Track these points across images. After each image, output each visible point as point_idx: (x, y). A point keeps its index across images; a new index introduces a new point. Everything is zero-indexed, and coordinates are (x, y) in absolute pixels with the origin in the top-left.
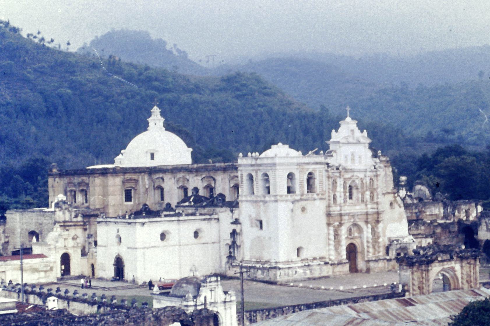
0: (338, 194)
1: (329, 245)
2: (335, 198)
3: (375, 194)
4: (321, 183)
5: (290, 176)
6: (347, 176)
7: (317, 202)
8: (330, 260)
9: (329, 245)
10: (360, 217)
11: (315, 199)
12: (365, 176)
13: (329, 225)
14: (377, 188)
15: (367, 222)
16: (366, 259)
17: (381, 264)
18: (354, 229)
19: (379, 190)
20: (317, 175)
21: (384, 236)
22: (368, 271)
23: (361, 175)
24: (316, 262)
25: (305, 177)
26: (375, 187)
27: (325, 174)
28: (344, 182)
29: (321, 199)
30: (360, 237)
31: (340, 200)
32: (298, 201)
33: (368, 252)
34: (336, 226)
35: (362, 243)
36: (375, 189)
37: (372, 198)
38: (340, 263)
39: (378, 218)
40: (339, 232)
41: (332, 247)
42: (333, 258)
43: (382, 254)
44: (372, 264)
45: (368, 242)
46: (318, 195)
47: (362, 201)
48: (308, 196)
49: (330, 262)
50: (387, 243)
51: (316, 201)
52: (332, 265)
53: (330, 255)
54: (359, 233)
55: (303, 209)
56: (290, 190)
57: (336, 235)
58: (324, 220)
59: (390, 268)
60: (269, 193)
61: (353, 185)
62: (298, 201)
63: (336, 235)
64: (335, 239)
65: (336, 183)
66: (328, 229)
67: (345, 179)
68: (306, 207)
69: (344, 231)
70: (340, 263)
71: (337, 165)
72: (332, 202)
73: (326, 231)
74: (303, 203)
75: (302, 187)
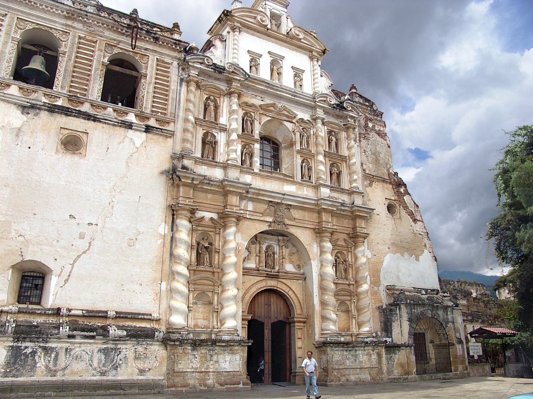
0: (221, 138)
1: (173, 274)
2: (209, 144)
4: (162, 91)
7: (138, 137)
9: (173, 274)
11: (129, 126)
13: (173, 211)
15: (319, 232)
16: (317, 337)
17: (365, 358)
21: (376, 282)
22: (324, 379)
23: (303, 115)
29: (148, 129)
30: (304, 278)
33: (324, 318)
35: (308, 295)
37: (336, 176)
38: (208, 343)
39: (354, 228)
42: (178, 320)
43: (369, 326)
44: (336, 355)
45: (323, 289)
46: (141, 116)
50: (385, 300)
53: (171, 310)
54: (299, 267)
57: (205, 252)
59: (396, 372)
62: (53, 109)
63: (205, 252)
65: (216, 107)
66: (173, 226)
68: (84, 137)
70: (208, 343)
73: (164, 229)
74: (76, 124)
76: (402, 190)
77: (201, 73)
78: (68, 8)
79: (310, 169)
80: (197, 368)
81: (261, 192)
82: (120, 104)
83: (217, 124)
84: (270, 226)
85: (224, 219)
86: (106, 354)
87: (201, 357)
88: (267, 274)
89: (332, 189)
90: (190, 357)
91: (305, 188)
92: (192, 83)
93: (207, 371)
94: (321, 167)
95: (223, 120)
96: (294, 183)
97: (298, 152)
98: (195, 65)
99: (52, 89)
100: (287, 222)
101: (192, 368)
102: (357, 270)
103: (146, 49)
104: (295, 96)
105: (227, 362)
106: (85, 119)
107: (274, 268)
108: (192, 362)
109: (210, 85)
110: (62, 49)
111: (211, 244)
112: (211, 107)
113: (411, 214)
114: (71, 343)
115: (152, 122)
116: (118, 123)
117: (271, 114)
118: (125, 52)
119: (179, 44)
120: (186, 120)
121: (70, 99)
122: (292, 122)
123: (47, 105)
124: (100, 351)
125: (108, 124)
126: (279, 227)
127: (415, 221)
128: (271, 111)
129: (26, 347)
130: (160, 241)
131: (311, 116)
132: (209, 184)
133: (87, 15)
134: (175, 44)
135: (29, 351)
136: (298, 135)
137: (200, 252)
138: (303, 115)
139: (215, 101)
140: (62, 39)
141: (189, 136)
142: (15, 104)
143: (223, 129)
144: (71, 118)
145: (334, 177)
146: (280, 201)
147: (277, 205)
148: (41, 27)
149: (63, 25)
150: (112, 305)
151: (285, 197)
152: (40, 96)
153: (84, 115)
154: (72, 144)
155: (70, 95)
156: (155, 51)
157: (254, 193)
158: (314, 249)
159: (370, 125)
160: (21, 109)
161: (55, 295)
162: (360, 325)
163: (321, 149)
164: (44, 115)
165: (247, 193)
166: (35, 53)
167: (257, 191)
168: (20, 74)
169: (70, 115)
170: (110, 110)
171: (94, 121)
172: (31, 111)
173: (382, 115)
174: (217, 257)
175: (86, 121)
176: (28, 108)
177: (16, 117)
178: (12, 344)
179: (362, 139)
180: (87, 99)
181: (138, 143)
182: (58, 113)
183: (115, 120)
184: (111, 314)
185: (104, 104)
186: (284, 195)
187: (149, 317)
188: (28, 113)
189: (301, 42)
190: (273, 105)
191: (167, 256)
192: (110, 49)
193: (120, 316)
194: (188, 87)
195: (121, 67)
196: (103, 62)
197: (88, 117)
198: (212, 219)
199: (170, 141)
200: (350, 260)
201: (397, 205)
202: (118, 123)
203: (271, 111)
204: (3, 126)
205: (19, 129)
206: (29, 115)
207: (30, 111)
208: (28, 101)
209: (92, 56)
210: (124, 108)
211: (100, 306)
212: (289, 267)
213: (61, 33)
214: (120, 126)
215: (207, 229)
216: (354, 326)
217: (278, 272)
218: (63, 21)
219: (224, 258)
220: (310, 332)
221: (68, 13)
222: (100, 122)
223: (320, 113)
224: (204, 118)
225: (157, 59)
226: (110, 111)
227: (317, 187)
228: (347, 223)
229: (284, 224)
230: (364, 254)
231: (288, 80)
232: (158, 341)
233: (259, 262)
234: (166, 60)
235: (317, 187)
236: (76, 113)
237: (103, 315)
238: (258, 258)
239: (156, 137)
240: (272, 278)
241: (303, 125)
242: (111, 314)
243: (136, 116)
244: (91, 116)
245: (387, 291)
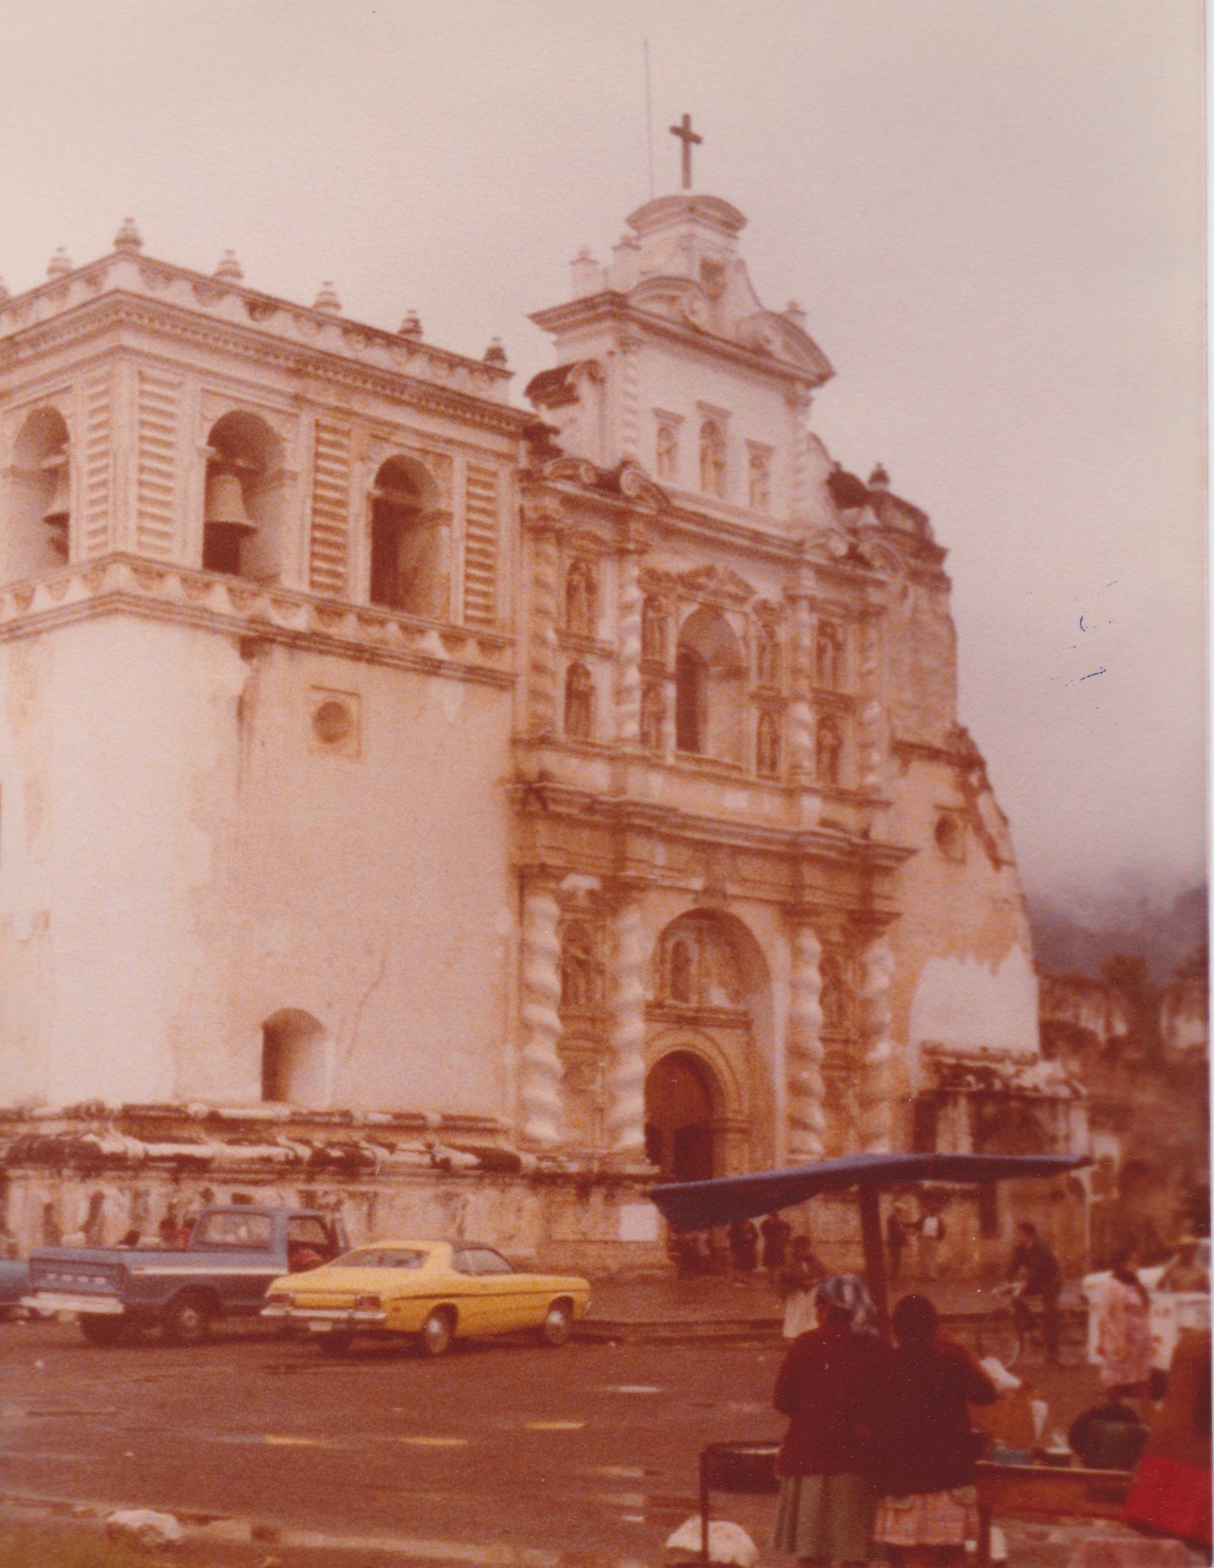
0: (602, 676)
2: (579, 696)
3: (849, 731)
5: (238, 450)
6: (675, 561)
7: (448, 695)
8: (528, 1142)
9: (527, 1028)
10: (749, 868)
11: (431, 667)
12: (793, 599)
13: (527, 877)
14: (866, 698)
15: (794, 914)
18: (704, 957)
19: (874, 711)
20: (452, 492)
24: (410, 1151)
25: (361, 483)
26: (850, 687)
27: (508, 498)
28: (650, 602)
29: (473, 675)
30: (744, 1022)
31: (616, 717)
32: (295, 642)
33: (798, 1124)
34: (582, 901)
36: (848, 704)
37: (829, 754)
38: (602, 1183)
39: (867, 896)
40: (603, 952)
41: (545, 1052)
42: (545, 1130)
45: (797, 1053)
46: (452, 638)
47: (767, 763)
48: (374, 632)
49: (529, 1160)
50: (919, 1079)
51: (435, 686)
52: (538, 1180)
53: (524, 1108)
54: (736, 996)
55: (331, 722)
56: (225, 549)
60: (61, 548)
61: (706, 648)
62: (295, 642)
64: (567, 998)
65: (591, 588)
66: (522, 914)
67: (652, 577)
68: (352, 705)
69: (636, 939)
70: (602, 1183)
71: (607, 463)
73: (504, 922)
74: (338, 673)
75: (326, 541)
76: (974, 779)
77: (570, 502)
78: (297, 350)
79: (775, 741)
84: (695, 901)
85: (618, 891)
89: (826, 797)
92: (548, 535)
94: (801, 730)
95: (605, 631)
96: (745, 785)
97: (754, 697)
100: (732, 889)
102: (867, 1004)
103: (449, 441)
107: (686, 1000)
111: (587, 950)
112: (580, 589)
113: (991, 847)
117: (701, 596)
120: (539, 640)
127: (997, 862)
128: (700, 588)
129: (326, 1193)
130: (499, 952)
131: (785, 589)
136: (754, 644)
138: (767, 588)
139: (587, 576)
141: (545, 684)
143: (607, 655)
145: (826, 756)
147: (704, 844)
156: (462, 445)
158: (777, 952)
162: (865, 1140)
163: (804, 686)
164: (279, 654)
165: (663, 824)
169: (329, 653)
171: (370, 661)
174: (599, 983)
184: (434, 1118)
185: (382, 611)
190: (710, 572)
191: (513, 985)
193: (452, 1125)
197: (359, 653)
198: (591, 893)
201: (960, 823)
203: (700, 588)
209: (344, 476)
211: (407, 1107)
212: (718, 998)
215: (581, 916)
217: (698, 1010)
219: (616, 985)
223: (809, 584)
224: (569, 627)
227: (791, 793)
228: (848, 885)
230: (881, 965)
232: (523, 1177)
235: (791, 793)
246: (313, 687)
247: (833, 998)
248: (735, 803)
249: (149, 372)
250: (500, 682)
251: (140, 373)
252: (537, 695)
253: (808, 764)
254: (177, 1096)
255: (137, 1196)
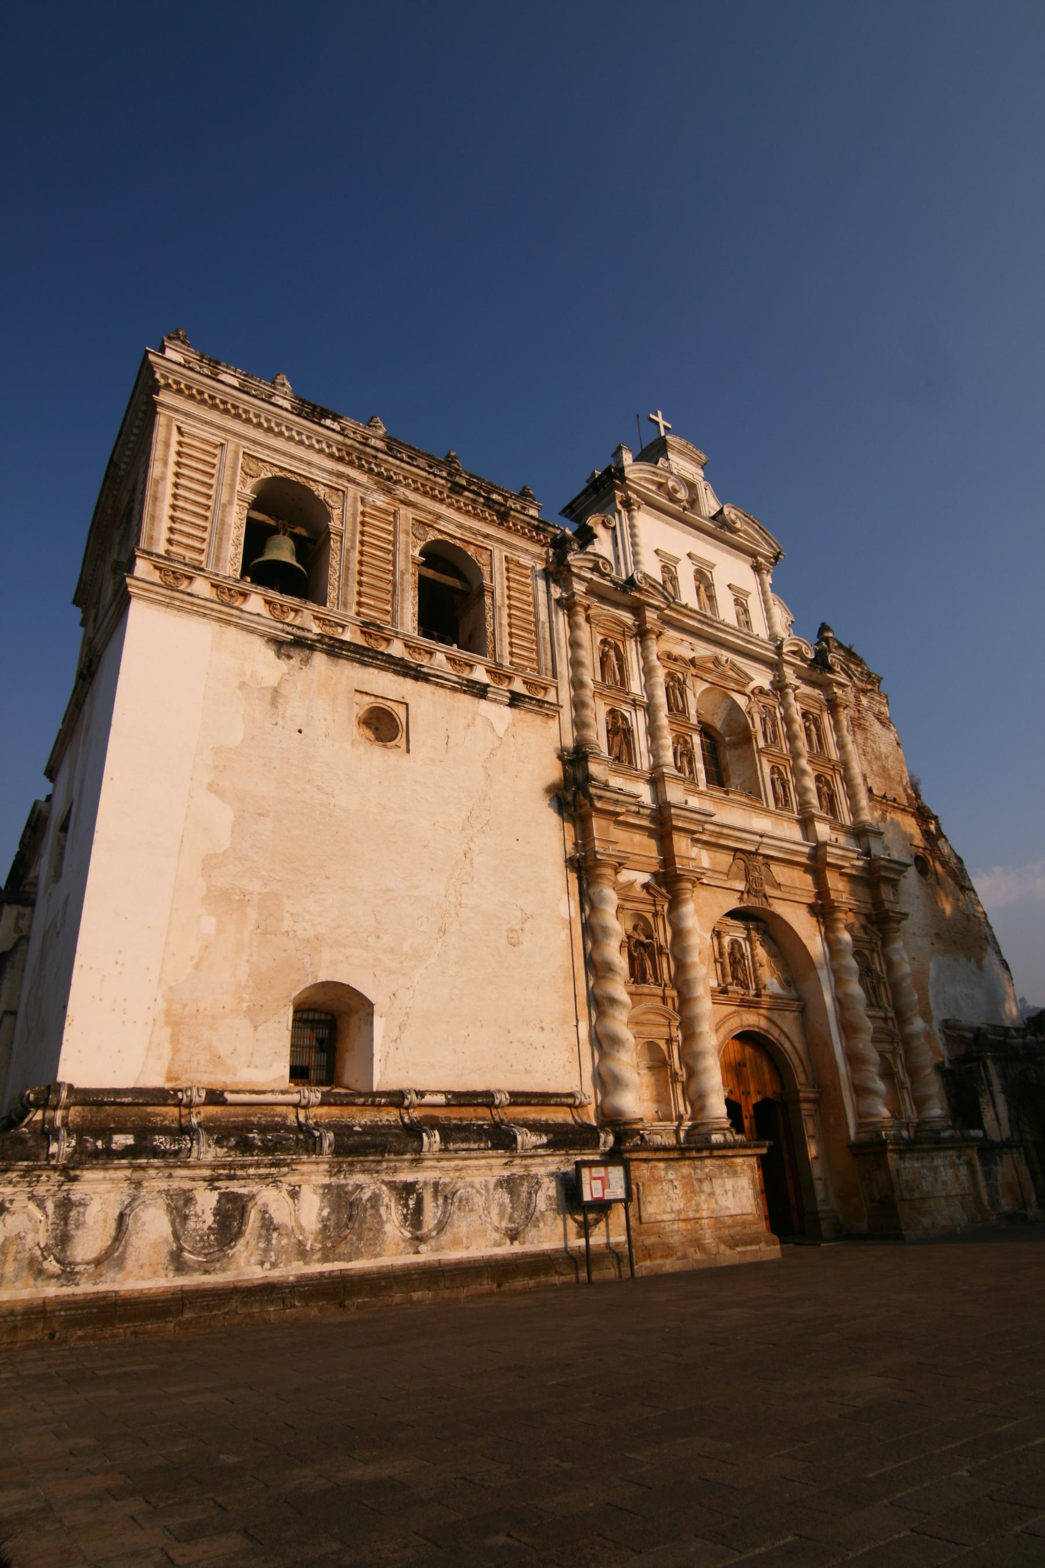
6: (685, 648)
7: (496, 714)
11: (480, 691)
45: (848, 1029)
46: (497, 673)
58: (550, 836)
62: (335, 649)
65: (621, 659)
68: (400, 711)
72: (599, 735)
73: (567, 907)
80: (679, 1212)
81: (726, 831)
82: (455, 645)
83: (627, 694)
84: (741, 899)
86: (511, 1192)
87: (685, 1185)
88: (742, 1000)
90: (666, 1186)
91: (785, 824)
93: (697, 1216)
95: (636, 686)
96: (767, 811)
98: (583, 574)
99: (325, 605)
101: (673, 1211)
103: (487, 536)
104: (748, 642)
105: (730, 1194)
106: (397, 673)
108: (669, 1198)
109: (606, 615)
110: (334, 525)
111: (649, 936)
114: (442, 1169)
115: (518, 686)
116: (461, 684)
118: (447, 538)
119: (544, 530)
121: (368, 627)
122: (744, 694)
123: (327, 640)
124: (499, 1184)
125: (442, 686)
126: (754, 902)
132: (638, 813)
133: (375, 457)
134: (537, 528)
135: (366, 1195)
137: (636, 954)
139: (616, 649)
140: (332, 504)
142: (262, 636)
144: (371, 670)
146: (753, 849)
148: (289, 475)
149: (331, 473)
150: (502, 1078)
151: (765, 840)
152: (307, 620)
153: (396, 665)
154: (382, 725)
155: (363, 623)
156: (502, 542)
157: (713, 832)
159: (864, 701)
160: (273, 647)
161: (404, 1057)
162: (920, 1103)
164: (319, 659)
166: (273, 531)
167: (717, 829)
168: (258, 570)
169: (370, 665)
170: (440, 657)
171: (416, 678)
172: (297, 655)
173: (879, 682)
175: (401, 679)
176: (292, 645)
177: (266, 665)
178: (327, 1180)
179: (856, 729)
180: (397, 633)
181: (500, 729)
182: (347, 658)
183: (456, 679)
186: (762, 836)
187: (570, 1101)
188: (290, 657)
189: (740, 536)
192: (421, 531)
193: (520, 1098)
194: (570, 617)
195: (437, 571)
196: (413, 557)
198: (646, 886)
199: (554, 724)
200: (878, 968)
202: (461, 684)
203: (709, 671)
204: (244, 683)
205: (276, 691)
206: (292, 662)
207: (293, 652)
208: (289, 629)
210: (465, 655)
213: (327, 490)
214: (465, 692)
216: (908, 1106)
218: (330, 464)
220: (832, 1121)
221: (339, 450)
222: (427, 681)
225: (506, 557)
226: (439, 658)
229: (765, 896)
231: (727, 612)
233: (724, 976)
234: (522, 561)
236: (381, 660)
237: (485, 1099)
238: (718, 965)
239: (530, 717)
240: (749, 1007)
241: (762, 699)
242: (502, 1098)
243: (488, 671)
244: (410, 668)
245: (947, 1031)
246: (356, 691)
247: (868, 980)
248: (761, 823)
249: (185, 428)
250: (546, 709)
251: (179, 428)
252: (580, 724)
253: (815, 801)
254: (169, 1079)
255: (66, 1206)
